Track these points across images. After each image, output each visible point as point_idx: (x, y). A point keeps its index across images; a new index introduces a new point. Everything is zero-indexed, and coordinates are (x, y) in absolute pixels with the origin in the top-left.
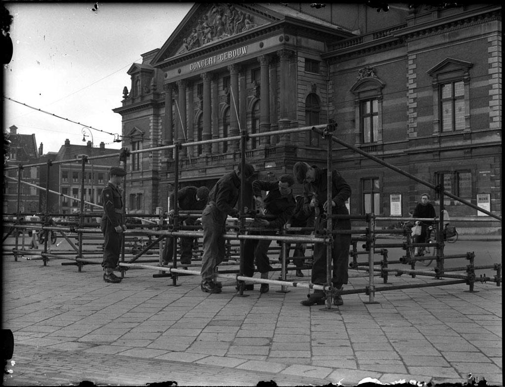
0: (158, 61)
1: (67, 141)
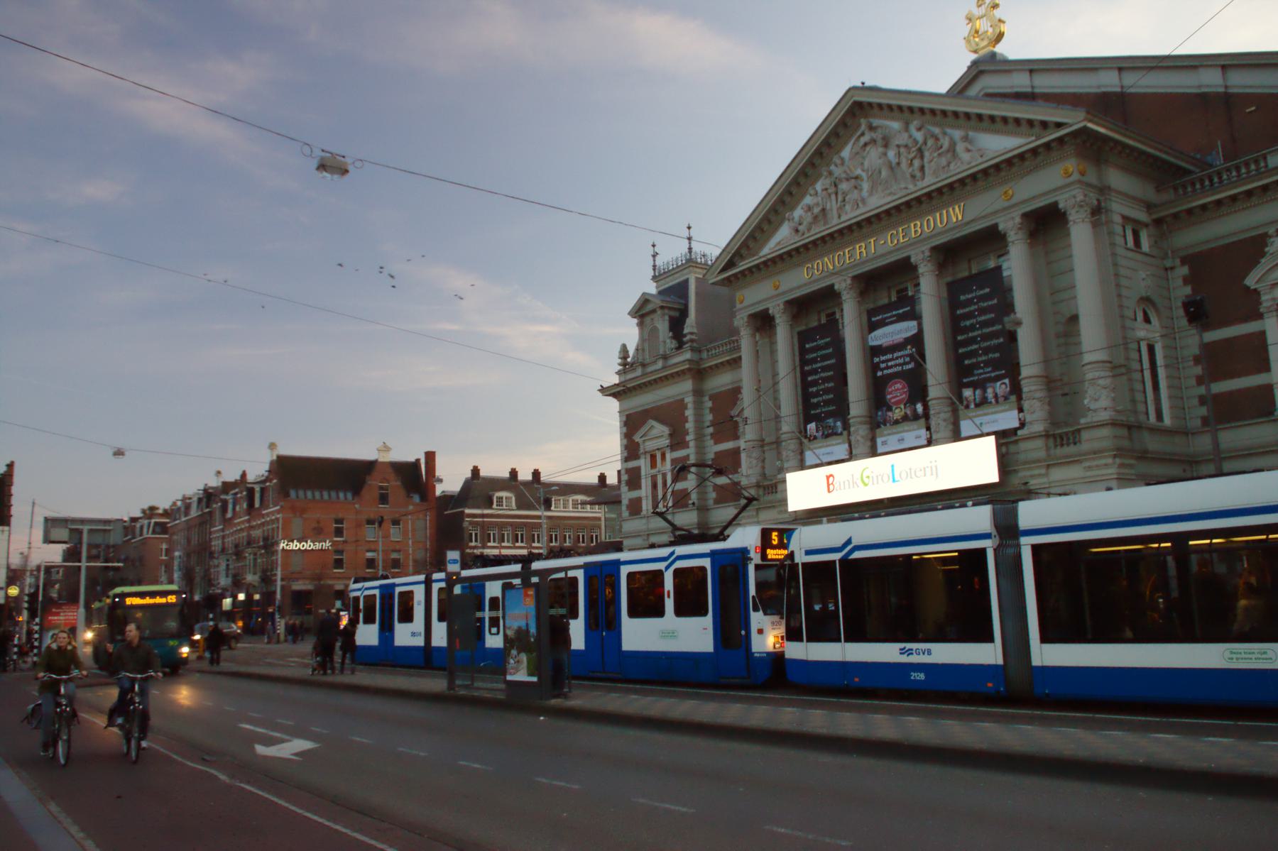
1: (475, 471)
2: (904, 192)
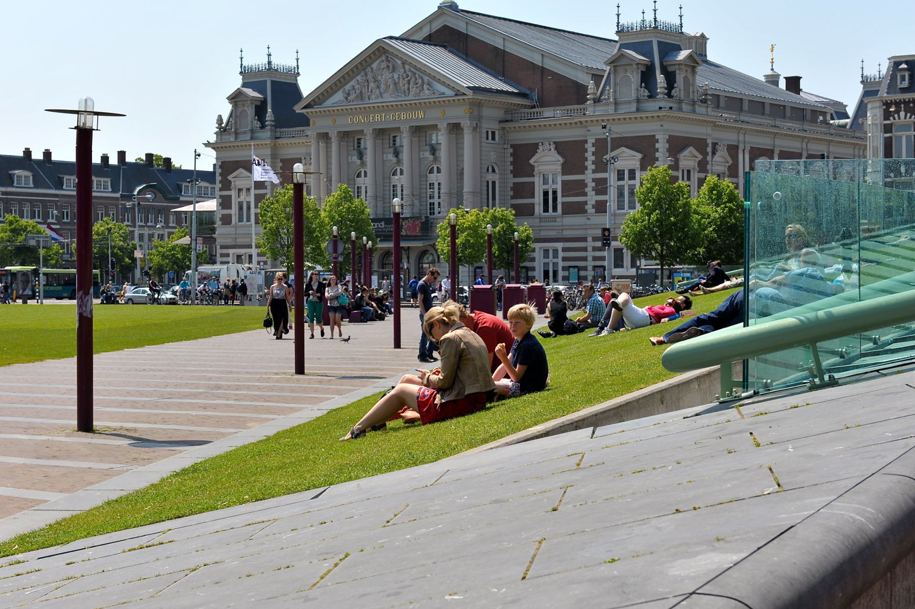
0: (305, 108)
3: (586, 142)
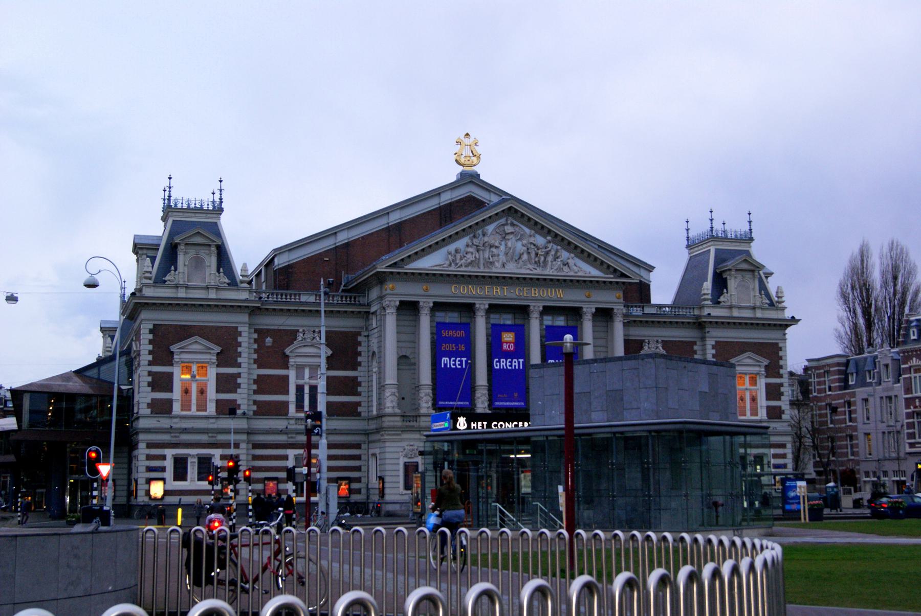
2: (535, 272)
3: (695, 343)
